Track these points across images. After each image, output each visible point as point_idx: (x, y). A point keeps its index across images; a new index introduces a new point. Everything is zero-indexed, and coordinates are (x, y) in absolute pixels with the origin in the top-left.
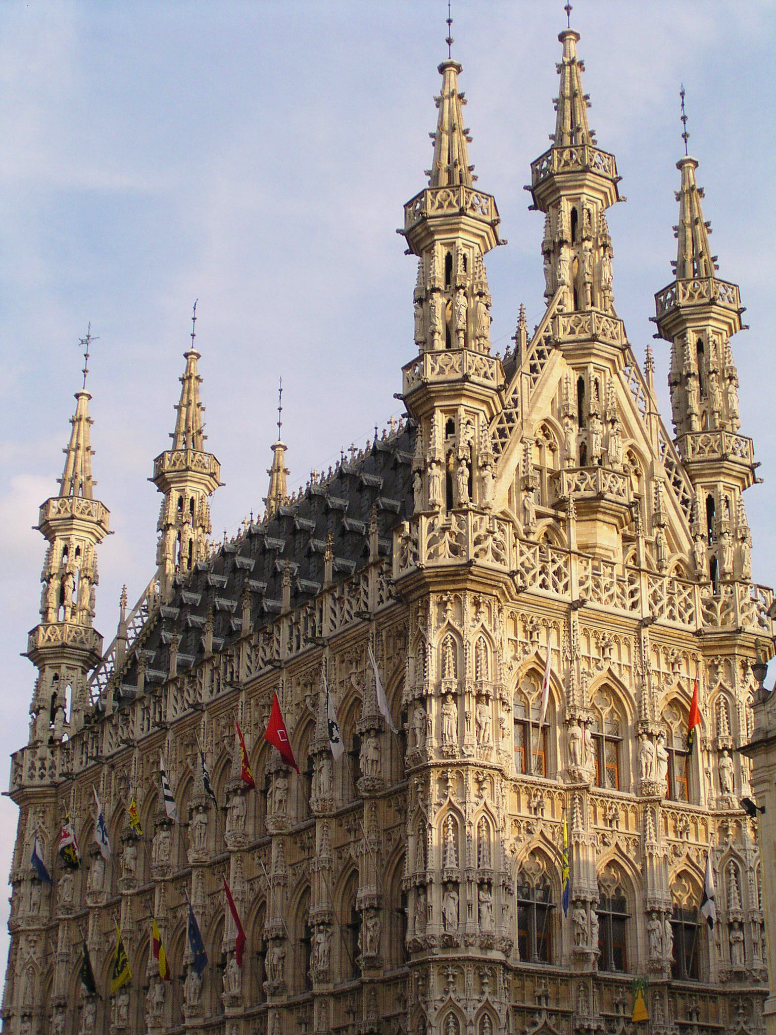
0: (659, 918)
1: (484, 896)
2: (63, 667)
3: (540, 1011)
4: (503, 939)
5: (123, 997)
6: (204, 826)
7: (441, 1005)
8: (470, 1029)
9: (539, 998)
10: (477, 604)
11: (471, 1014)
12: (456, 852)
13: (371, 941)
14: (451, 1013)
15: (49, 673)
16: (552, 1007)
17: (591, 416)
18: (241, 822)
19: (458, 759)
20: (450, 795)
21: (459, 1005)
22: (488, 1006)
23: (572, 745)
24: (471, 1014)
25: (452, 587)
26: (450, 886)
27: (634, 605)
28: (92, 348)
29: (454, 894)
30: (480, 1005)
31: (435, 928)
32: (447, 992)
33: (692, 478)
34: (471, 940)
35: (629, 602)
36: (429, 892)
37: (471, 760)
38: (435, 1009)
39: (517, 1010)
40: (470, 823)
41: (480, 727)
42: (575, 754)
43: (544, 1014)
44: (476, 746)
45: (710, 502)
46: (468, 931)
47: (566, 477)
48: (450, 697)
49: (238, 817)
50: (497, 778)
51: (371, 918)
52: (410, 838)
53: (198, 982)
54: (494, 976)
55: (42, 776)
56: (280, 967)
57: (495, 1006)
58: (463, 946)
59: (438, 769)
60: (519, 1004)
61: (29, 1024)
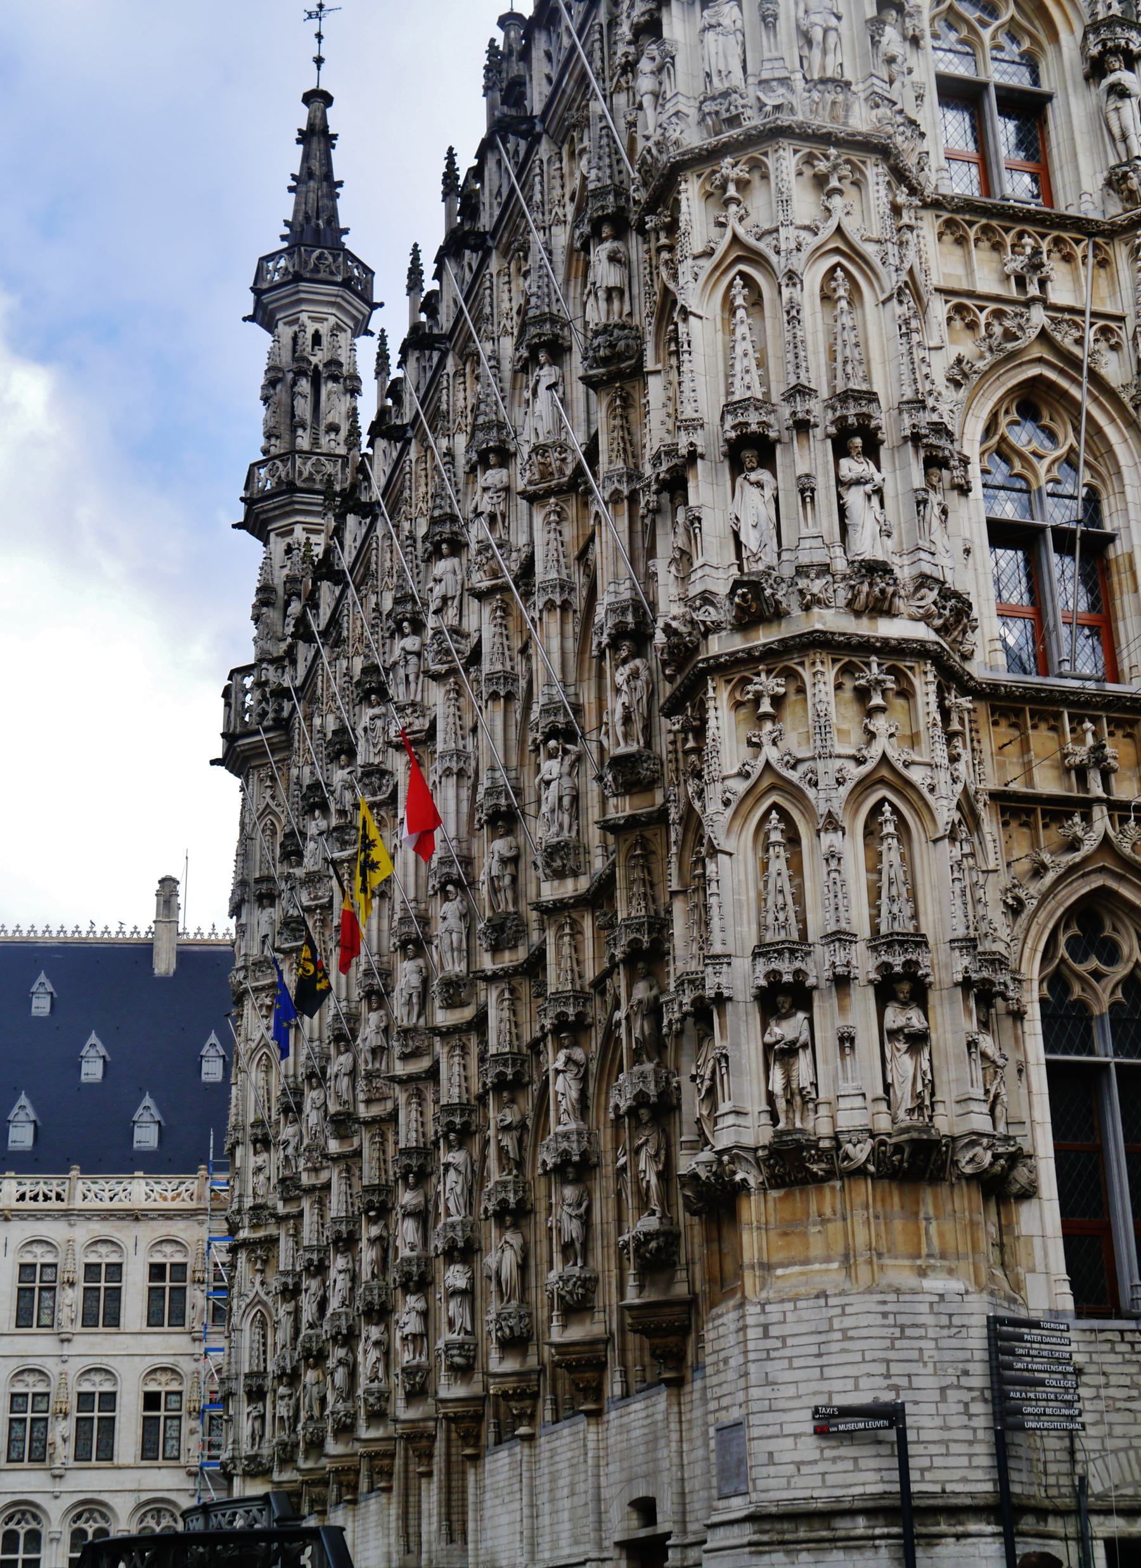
1: (851, 467)
2: (298, 528)
3: (1085, 806)
4: (924, 581)
5: (342, 1059)
6: (413, 660)
7: (740, 787)
8: (829, 839)
9: (1081, 772)
11: (828, 798)
12: (761, 364)
13: (627, 720)
14: (775, 806)
15: (278, 545)
18: (452, 611)
19: (753, 121)
20: (733, 222)
21: (794, 776)
22: (887, 776)
23: (1113, 117)
26: (749, 456)
28: (328, 25)
29: (763, 475)
34: (816, 586)
36: (691, 485)
37: (785, 119)
38: (727, 803)
39: (1015, 807)
40: (791, 275)
41: (809, 42)
42: (1125, 138)
43: (1101, 820)
44: (799, 84)
46: (804, 559)
49: (445, 599)
50: (875, 173)
51: (625, 661)
52: (652, 381)
53: (415, 980)
54: (906, 693)
55: (263, 715)
56: (507, 880)
57: (916, 775)
58: (796, 612)
59: (698, 169)
60: (1017, 787)
61: (265, 1155)
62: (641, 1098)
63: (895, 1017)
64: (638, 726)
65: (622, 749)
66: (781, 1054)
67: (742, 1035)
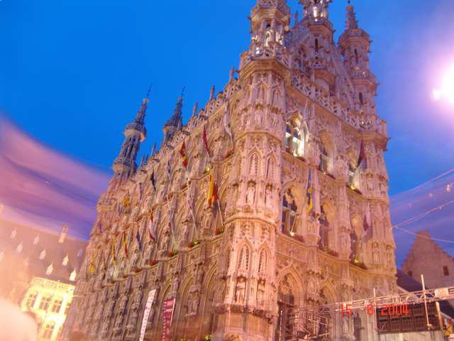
0: (345, 231)
10: (274, 78)
13: (208, 222)
16: (295, 258)
17: (321, 47)
20: (255, 146)
24: (256, 246)
25: (265, 68)
27: (335, 112)
30: (261, 243)
31: (241, 202)
32: (244, 234)
33: (354, 85)
35: (333, 110)
45: (361, 95)
47: (310, 63)
48: (259, 107)
62: (197, 291)
63: (260, 287)
64: (209, 224)
65: (206, 227)
66: (236, 289)
67: (232, 284)
